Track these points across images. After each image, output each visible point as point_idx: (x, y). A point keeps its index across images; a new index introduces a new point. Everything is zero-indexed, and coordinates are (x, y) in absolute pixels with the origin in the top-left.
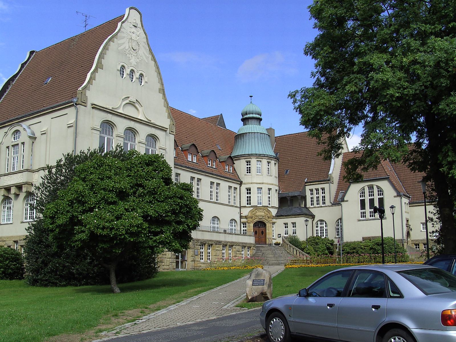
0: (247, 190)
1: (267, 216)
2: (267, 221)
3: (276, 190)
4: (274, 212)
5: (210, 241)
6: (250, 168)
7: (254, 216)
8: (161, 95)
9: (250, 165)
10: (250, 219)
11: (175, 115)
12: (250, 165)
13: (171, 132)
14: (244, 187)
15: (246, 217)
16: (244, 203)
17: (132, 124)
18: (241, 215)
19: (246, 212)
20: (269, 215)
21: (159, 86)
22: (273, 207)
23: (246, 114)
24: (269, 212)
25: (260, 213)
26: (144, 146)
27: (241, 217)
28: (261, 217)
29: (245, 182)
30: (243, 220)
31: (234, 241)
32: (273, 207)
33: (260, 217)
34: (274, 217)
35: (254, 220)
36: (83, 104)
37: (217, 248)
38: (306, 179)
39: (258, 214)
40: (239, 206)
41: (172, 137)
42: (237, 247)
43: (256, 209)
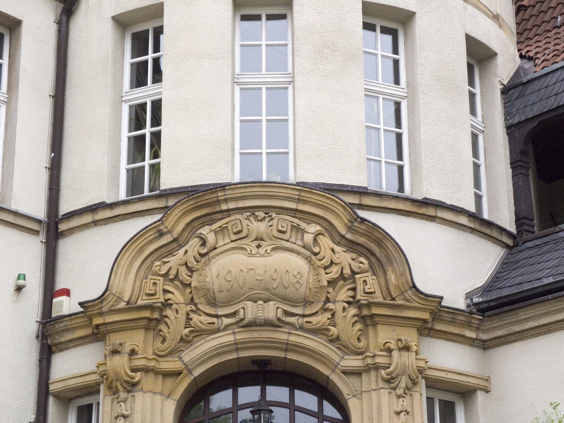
1: (344, 294)
2: (353, 362)
3: (479, 56)
7: (177, 296)
10: (135, 339)
19: (91, 265)
20: (369, 283)
22: (426, 209)
24: (378, 250)
25: (256, 264)
28: (271, 311)
30: (74, 365)
32: (426, 209)
33: (251, 310)
35: (191, 354)
39: (231, 266)
40: (39, 210)
43: (208, 219)
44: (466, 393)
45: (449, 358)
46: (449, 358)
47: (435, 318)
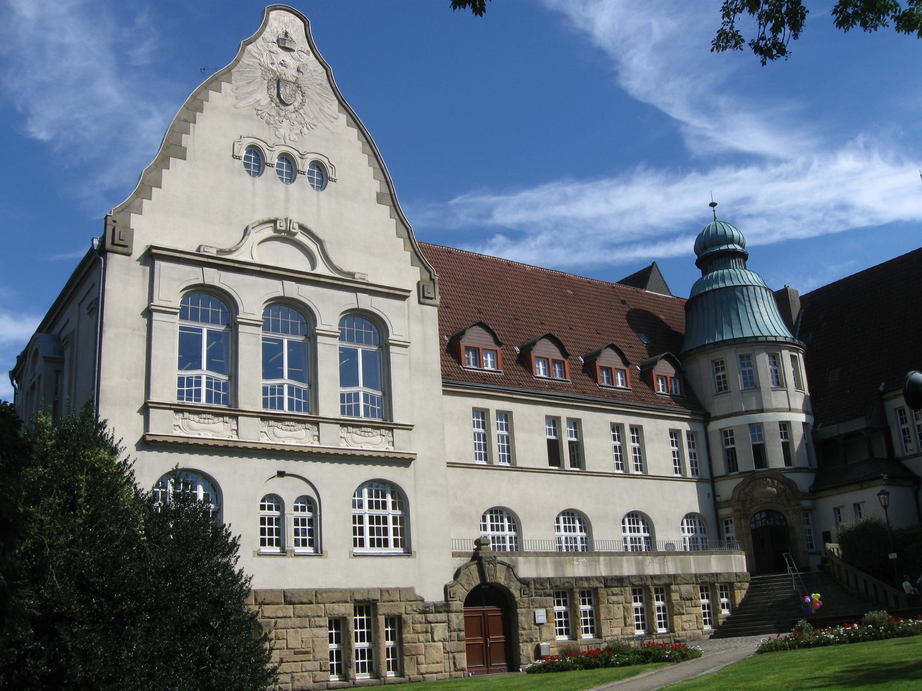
0: (726, 435)
4: (803, 482)
5: (587, 579)
6: (724, 376)
8: (386, 210)
9: (723, 369)
11: (425, 253)
12: (723, 369)
13: (422, 300)
14: (715, 426)
15: (728, 503)
16: (720, 467)
17: (292, 290)
18: (718, 499)
21: (375, 186)
22: (798, 470)
23: (705, 248)
24: (790, 484)
26: (336, 341)
27: (717, 506)
29: (718, 414)
31: (671, 571)
32: (798, 470)
34: (804, 496)
36: (120, 249)
37: (614, 598)
38: (883, 384)
41: (432, 313)
42: (685, 589)
44: (811, 510)
45: (806, 503)
46: (806, 503)
47: (804, 496)
